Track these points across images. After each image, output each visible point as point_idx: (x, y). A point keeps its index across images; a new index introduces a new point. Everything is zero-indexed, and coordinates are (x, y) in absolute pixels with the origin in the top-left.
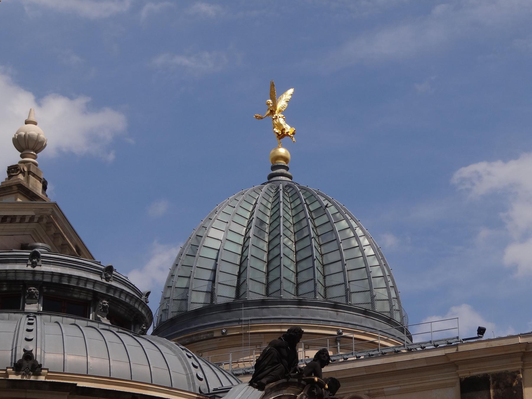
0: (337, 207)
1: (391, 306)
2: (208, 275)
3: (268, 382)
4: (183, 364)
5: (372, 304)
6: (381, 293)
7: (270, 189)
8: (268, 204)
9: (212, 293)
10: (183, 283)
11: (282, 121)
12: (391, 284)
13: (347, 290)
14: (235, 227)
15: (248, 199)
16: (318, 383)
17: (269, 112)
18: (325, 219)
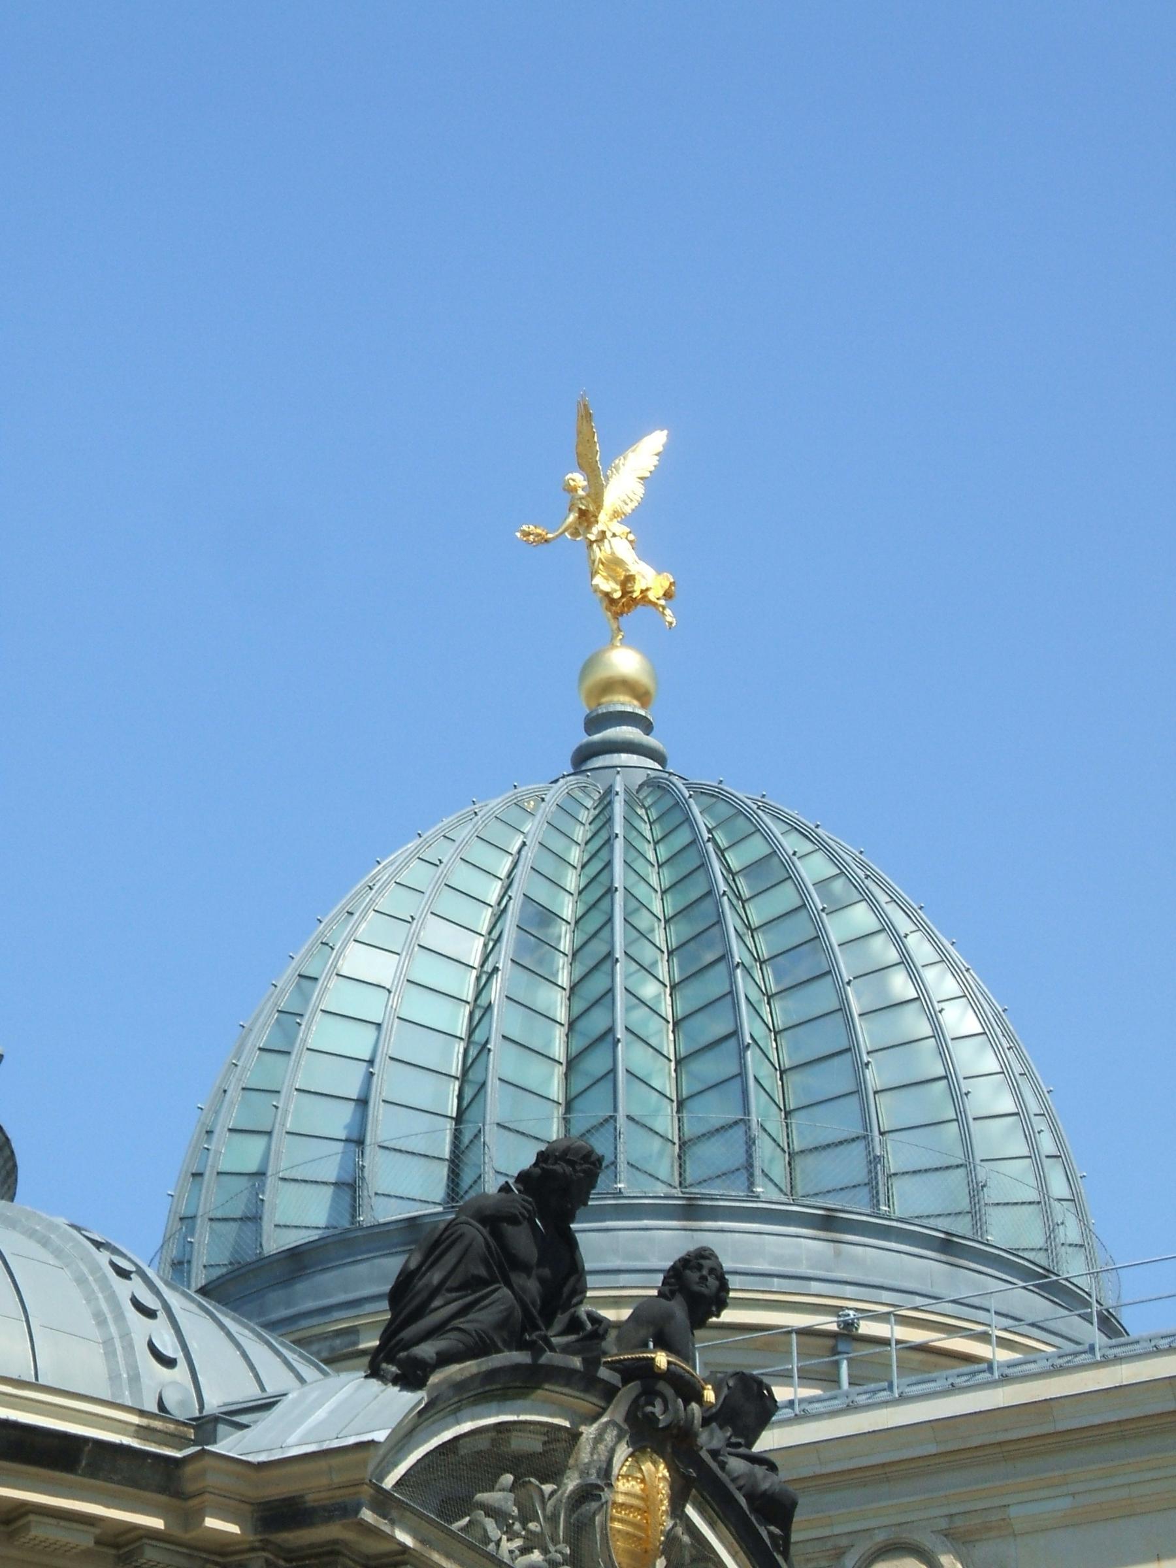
0: (832, 857)
1: (1051, 1229)
2: (338, 1121)
3: (445, 1359)
4: (90, 1298)
5: (975, 1212)
6: (1011, 1180)
7: (579, 794)
8: (569, 849)
9: (350, 1187)
10: (245, 1155)
11: (621, 548)
12: (1047, 1144)
13: (875, 1161)
14: (437, 934)
15: (496, 832)
16: (671, 1376)
17: (572, 517)
18: (786, 897)
